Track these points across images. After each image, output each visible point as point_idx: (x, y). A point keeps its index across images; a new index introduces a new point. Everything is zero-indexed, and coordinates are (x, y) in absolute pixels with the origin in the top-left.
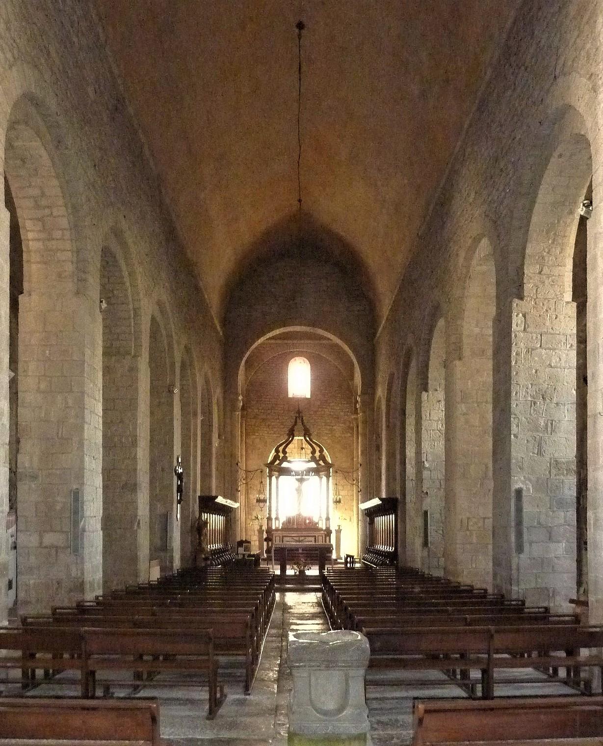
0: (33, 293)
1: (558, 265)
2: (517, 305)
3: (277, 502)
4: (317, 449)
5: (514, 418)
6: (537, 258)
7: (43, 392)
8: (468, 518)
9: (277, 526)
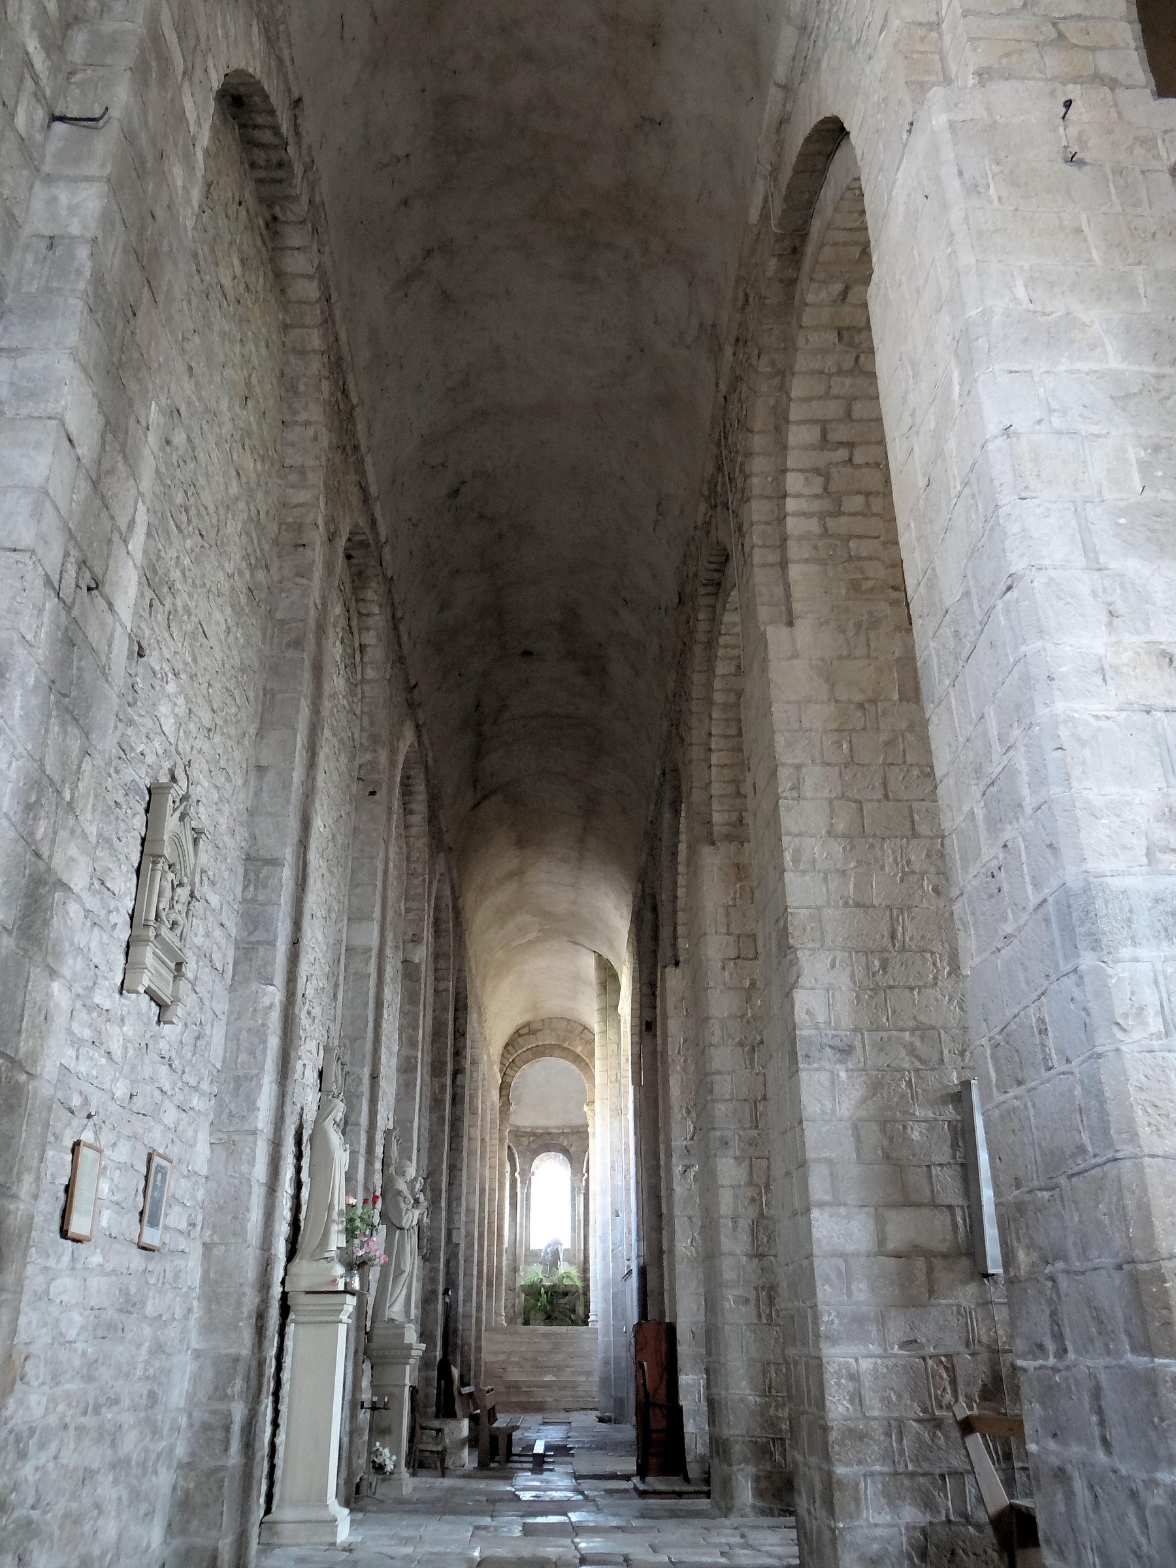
0: (798, 622)
7: (844, 836)
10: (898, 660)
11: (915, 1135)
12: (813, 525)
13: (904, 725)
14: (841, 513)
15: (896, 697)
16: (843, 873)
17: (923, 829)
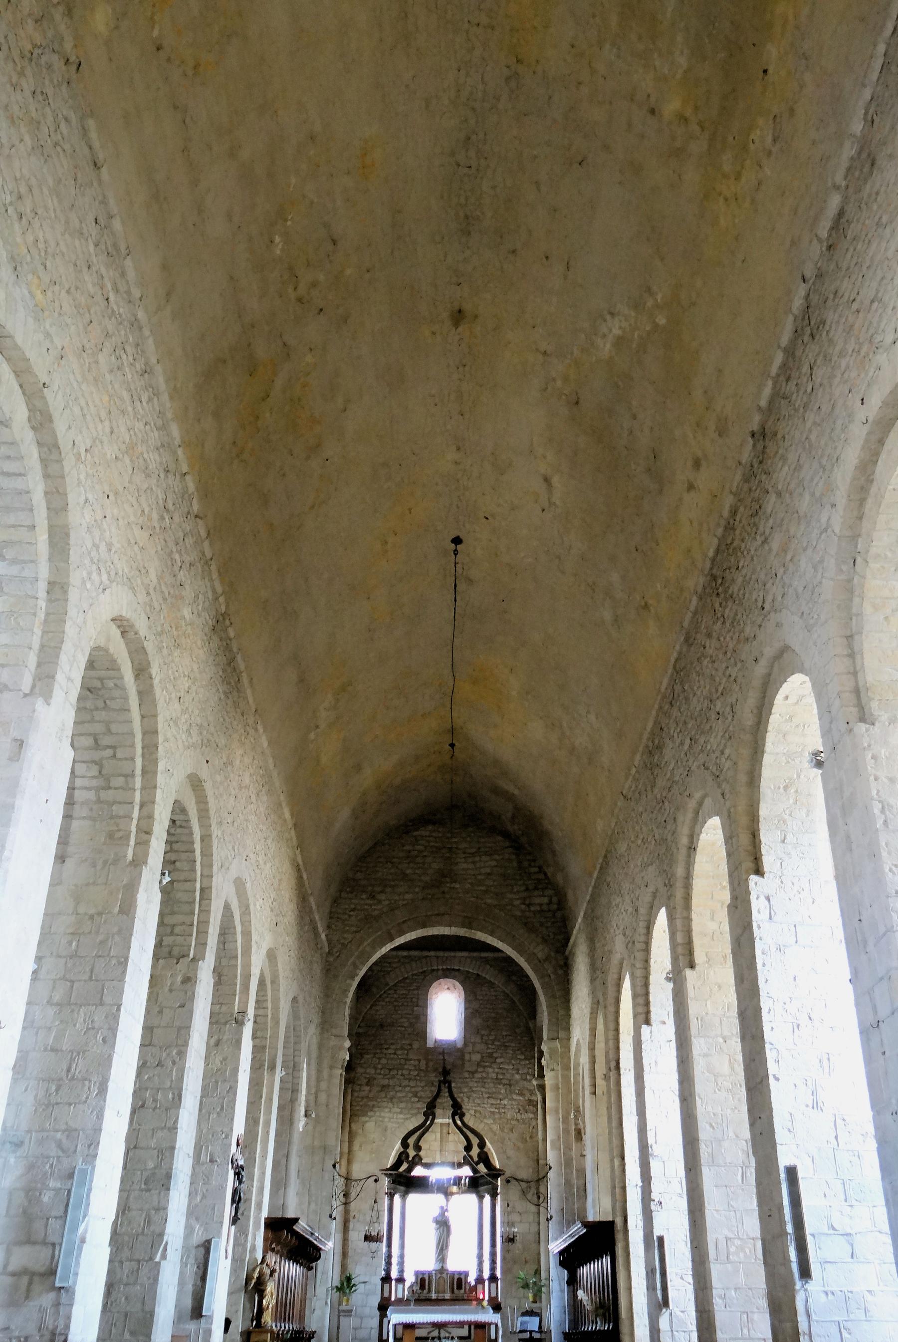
0: (68, 860)
1: (807, 832)
2: (756, 884)
3: (402, 1246)
4: (475, 1141)
5: (771, 1049)
6: (776, 822)
7: (57, 1004)
8: (727, 1239)
9: (400, 1296)
10: (124, 886)
11: (45, 1199)
12: (91, 795)
13: (116, 929)
14: (110, 788)
15: (117, 909)
16: (50, 1029)
17: (107, 999)
